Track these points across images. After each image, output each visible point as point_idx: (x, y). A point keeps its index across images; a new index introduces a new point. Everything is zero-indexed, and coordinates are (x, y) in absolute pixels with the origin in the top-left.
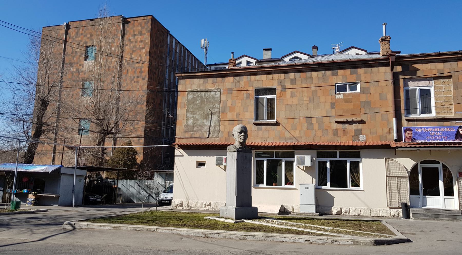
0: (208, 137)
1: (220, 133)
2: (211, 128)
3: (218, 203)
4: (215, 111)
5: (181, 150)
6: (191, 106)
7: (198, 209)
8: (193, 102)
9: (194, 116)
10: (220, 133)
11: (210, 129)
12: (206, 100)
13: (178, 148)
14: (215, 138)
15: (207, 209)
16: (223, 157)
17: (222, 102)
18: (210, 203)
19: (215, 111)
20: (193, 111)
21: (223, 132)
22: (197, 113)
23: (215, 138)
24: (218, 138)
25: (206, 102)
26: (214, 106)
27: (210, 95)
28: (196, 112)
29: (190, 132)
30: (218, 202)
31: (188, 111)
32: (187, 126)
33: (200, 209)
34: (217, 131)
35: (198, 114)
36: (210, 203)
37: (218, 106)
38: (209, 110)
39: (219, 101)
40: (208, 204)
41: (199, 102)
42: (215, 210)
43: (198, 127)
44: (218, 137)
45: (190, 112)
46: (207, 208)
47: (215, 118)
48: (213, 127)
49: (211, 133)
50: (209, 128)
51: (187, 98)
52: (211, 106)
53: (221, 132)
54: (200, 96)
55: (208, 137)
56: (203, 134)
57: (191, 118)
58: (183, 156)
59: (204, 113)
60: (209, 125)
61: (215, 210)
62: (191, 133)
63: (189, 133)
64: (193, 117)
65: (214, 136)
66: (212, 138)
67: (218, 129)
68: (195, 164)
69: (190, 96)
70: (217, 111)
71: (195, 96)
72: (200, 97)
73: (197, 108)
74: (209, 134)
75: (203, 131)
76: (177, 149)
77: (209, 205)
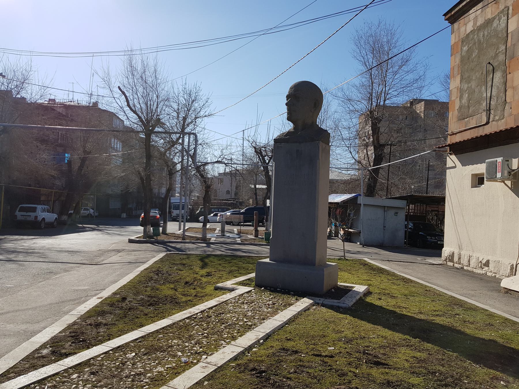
0: (487, 123)
1: (505, 108)
2: (491, 103)
3: (500, 262)
4: (498, 61)
5: (453, 157)
6: (466, 68)
7: (472, 270)
8: (469, 59)
9: (470, 85)
10: (507, 107)
11: (490, 103)
12: (485, 46)
13: (450, 154)
14: (498, 120)
15: (484, 272)
16: (497, 161)
17: (510, 35)
18: (488, 261)
19: (498, 62)
20: (469, 77)
21: (510, 102)
22: (474, 79)
23: (498, 120)
24: (502, 121)
25: (486, 49)
26: (498, 51)
27: (491, 31)
28: (472, 77)
29: (464, 119)
30: (501, 259)
31: (463, 79)
32: (460, 107)
33: (474, 270)
34: (501, 104)
35: (474, 79)
36: (488, 261)
37: (504, 47)
38: (489, 63)
39: (505, 35)
40: (484, 262)
41: (476, 54)
42: (495, 276)
43: (474, 107)
44: (503, 119)
45: (465, 78)
46: (484, 269)
47: (498, 75)
48: (495, 98)
49: (492, 112)
50: (488, 102)
51: (461, 54)
52: (492, 53)
53: (507, 104)
54: (476, 41)
55: (487, 123)
56: (481, 118)
57: (465, 92)
58: (455, 167)
59: (482, 73)
60: (489, 95)
61: (495, 276)
62: (466, 120)
63: (463, 121)
64: (468, 87)
65: (497, 118)
66: (494, 122)
67: (504, 98)
68: (468, 182)
69: (464, 49)
70: (501, 60)
71: (470, 46)
72: (477, 44)
73: (472, 68)
74: (490, 114)
75: (480, 111)
76: (449, 156)
77: (487, 264)
